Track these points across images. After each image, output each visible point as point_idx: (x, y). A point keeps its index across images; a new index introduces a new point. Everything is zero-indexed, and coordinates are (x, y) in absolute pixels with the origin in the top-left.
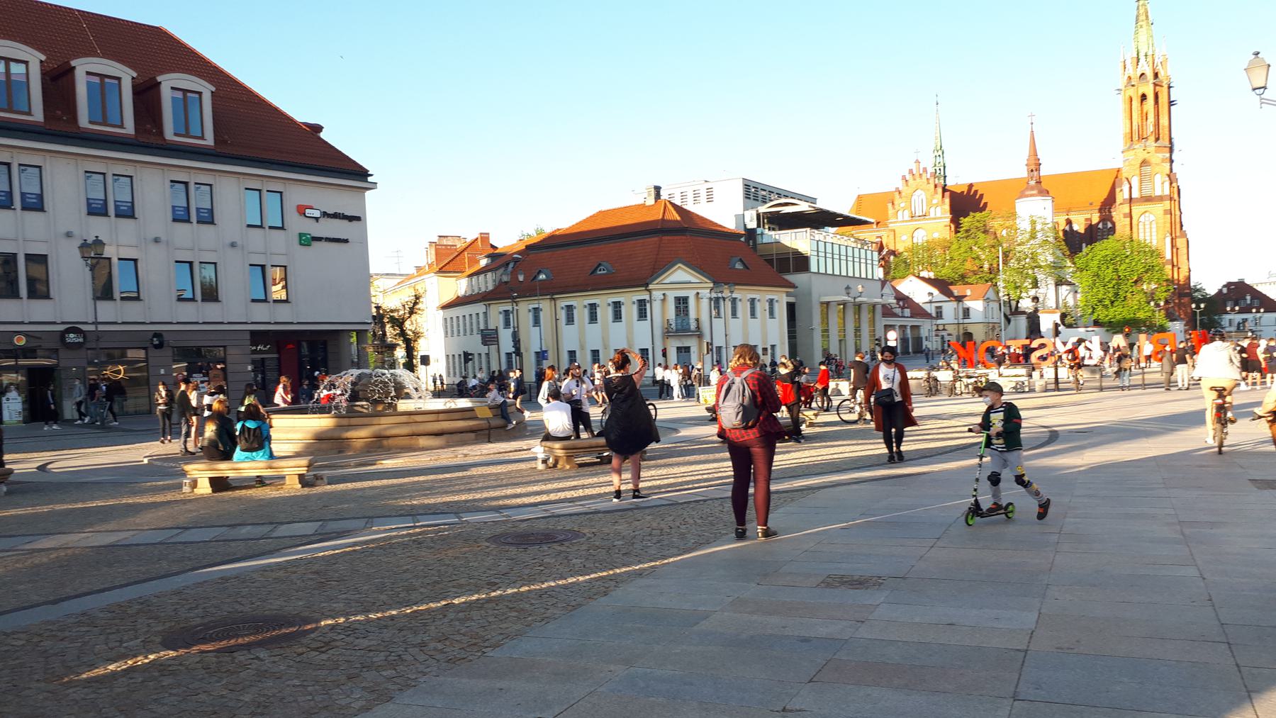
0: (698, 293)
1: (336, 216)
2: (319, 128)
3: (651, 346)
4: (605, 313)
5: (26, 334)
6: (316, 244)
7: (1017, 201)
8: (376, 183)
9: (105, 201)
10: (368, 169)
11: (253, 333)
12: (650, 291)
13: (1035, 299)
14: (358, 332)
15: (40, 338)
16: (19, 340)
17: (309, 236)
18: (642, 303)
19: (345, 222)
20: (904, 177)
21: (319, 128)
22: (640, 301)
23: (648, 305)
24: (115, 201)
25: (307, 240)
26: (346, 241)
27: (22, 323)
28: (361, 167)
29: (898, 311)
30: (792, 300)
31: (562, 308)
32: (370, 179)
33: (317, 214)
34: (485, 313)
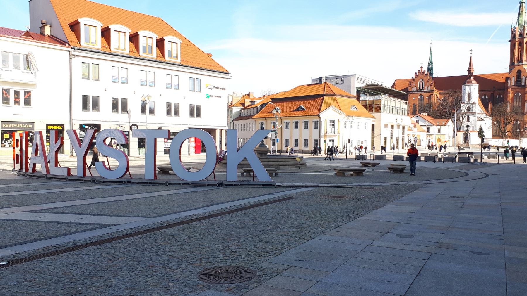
0: (339, 119)
2: (210, 55)
3: (319, 139)
4: (301, 125)
7: (463, 85)
12: (320, 118)
17: (209, 95)
18: (316, 122)
20: (416, 73)
21: (210, 55)
22: (316, 122)
23: (319, 123)
25: (208, 96)
29: (413, 129)
30: (373, 123)
31: (284, 123)
33: (212, 87)
34: (254, 124)
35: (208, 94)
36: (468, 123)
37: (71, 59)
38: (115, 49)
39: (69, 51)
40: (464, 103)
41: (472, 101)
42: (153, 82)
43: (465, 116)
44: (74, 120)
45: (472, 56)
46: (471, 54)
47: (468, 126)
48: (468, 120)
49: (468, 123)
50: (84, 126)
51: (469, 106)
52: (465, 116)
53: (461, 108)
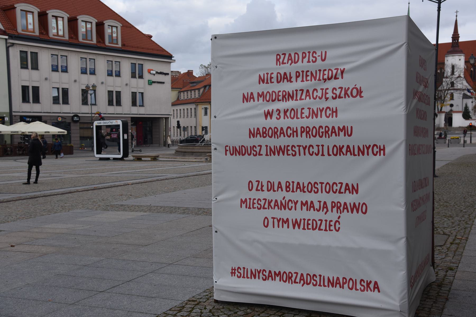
1: (161, 73)
5: (62, 117)
6: (154, 84)
7: (446, 56)
8: (175, 60)
9: (86, 68)
10: (172, 54)
11: (132, 118)
13: (452, 105)
14: (166, 118)
15: (65, 118)
16: (60, 119)
17: (151, 81)
19: (164, 76)
21: (151, 37)
24: (90, 68)
26: (163, 83)
27: (41, 112)
28: (170, 54)
32: (173, 58)
33: (154, 72)
35: (150, 81)
36: (452, 102)
37: (9, 47)
38: (54, 35)
39: (6, 39)
40: (447, 77)
41: (457, 74)
42: (94, 70)
43: (447, 94)
44: (14, 112)
45: (457, 19)
46: (457, 16)
47: (452, 105)
48: (452, 98)
49: (452, 102)
50: (24, 118)
51: (452, 81)
52: (447, 94)
53: (443, 83)
